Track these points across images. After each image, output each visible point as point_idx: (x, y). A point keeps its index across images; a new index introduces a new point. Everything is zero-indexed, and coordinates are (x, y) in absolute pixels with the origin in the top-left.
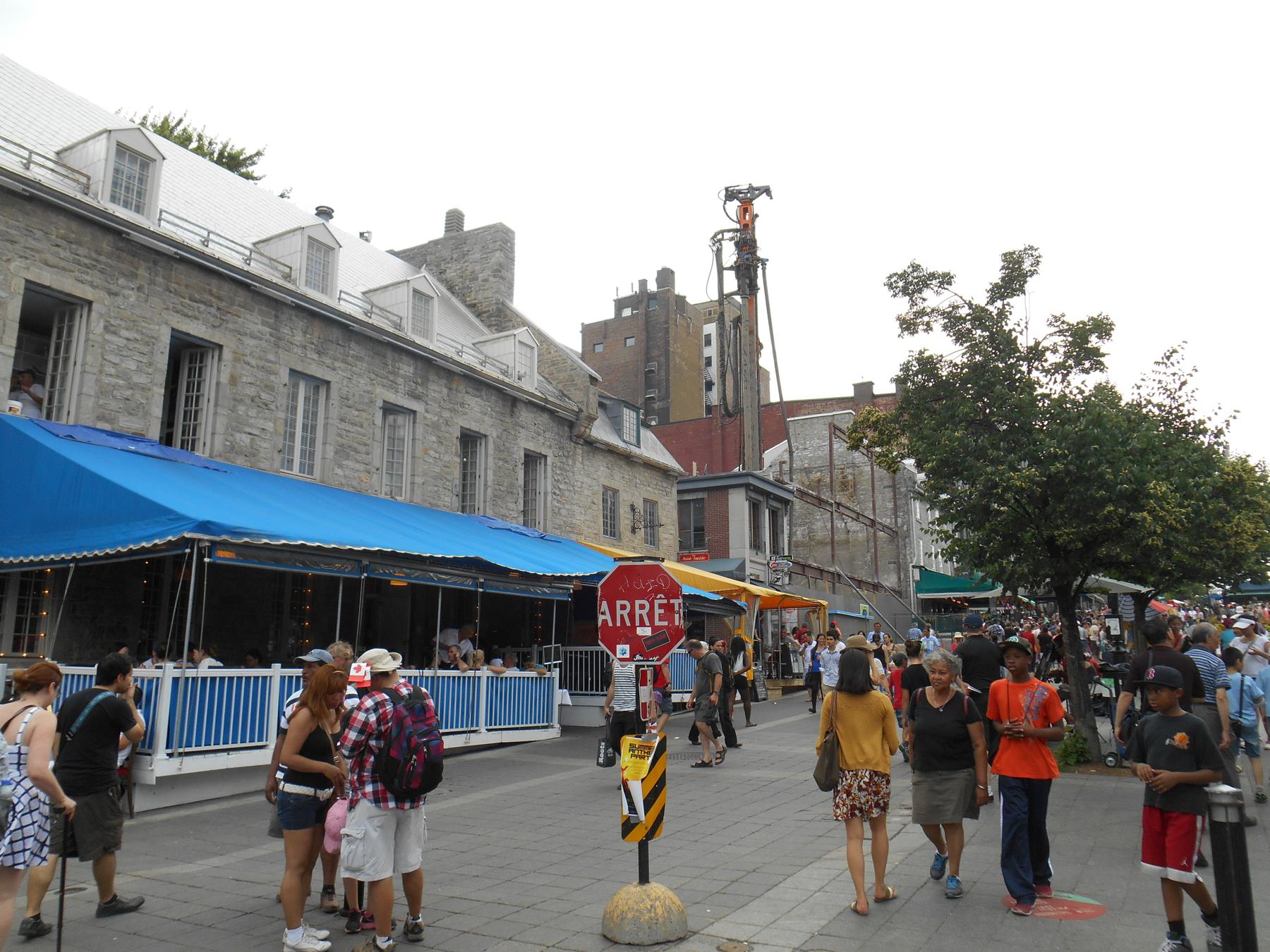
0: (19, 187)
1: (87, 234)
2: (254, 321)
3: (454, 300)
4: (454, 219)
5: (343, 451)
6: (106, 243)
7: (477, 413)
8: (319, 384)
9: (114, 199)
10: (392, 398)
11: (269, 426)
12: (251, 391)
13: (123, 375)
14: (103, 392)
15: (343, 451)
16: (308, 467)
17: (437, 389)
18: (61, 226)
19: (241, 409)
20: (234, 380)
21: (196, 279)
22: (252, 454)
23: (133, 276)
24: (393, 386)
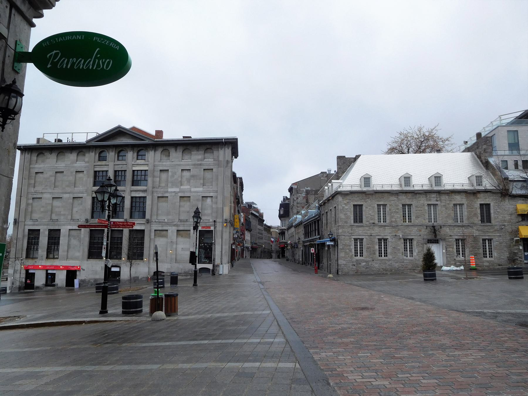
0: (348, 192)
1: (360, 195)
2: (393, 198)
3: (478, 160)
4: (479, 135)
5: (417, 217)
6: (364, 195)
7: (458, 199)
8: (410, 205)
9: (365, 186)
10: (430, 203)
11: (399, 216)
12: (394, 210)
13: (370, 214)
14: (367, 218)
15: (417, 217)
16: (410, 221)
17: (444, 197)
18: (356, 195)
19: (392, 214)
20: (390, 210)
21: (380, 195)
22: (396, 221)
23: (369, 198)
24: (430, 200)
